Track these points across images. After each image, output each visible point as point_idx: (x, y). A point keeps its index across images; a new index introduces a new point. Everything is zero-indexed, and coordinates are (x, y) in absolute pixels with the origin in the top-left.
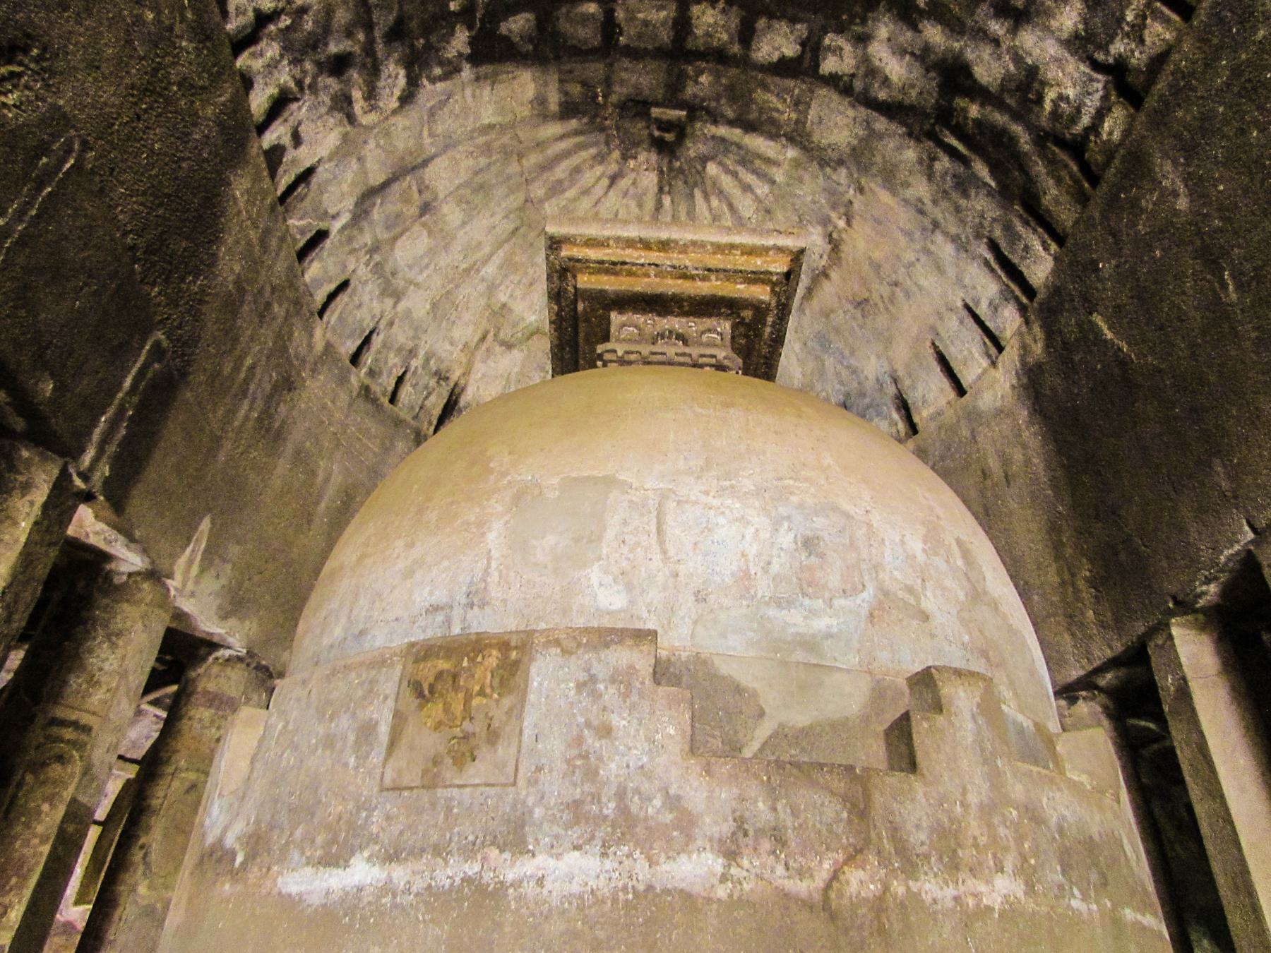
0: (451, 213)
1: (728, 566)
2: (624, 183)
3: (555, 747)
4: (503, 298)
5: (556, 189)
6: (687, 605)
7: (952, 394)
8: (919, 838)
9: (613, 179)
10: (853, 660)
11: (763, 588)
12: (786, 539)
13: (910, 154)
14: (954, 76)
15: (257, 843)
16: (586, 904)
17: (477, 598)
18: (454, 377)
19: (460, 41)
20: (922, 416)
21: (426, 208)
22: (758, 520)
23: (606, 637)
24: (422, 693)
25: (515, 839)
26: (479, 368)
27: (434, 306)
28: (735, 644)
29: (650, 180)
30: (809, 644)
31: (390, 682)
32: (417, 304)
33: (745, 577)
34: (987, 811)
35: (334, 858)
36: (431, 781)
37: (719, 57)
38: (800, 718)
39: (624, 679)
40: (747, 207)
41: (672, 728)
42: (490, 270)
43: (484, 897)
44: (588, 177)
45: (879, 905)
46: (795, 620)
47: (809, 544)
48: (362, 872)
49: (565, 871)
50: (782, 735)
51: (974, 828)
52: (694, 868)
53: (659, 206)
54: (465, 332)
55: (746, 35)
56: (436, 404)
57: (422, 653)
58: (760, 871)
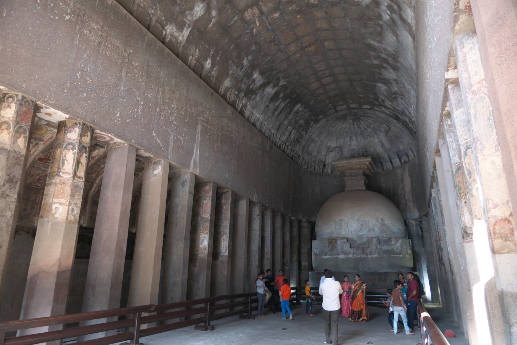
0: (317, 139)
1: (354, 229)
2: (346, 122)
3: (340, 248)
4: (328, 145)
5: (333, 127)
6: (350, 233)
7: (413, 157)
8: (368, 253)
9: (343, 123)
10: (365, 237)
11: (357, 231)
12: (359, 225)
13: (395, 121)
14: (396, 116)
15: (320, 254)
16: (343, 258)
17: (332, 233)
18: (324, 160)
19: (312, 123)
20: (410, 158)
21: (313, 141)
22: (357, 223)
23: (343, 238)
24: (330, 243)
25: (338, 254)
26: (327, 157)
27: (317, 152)
28: (355, 236)
29: (351, 121)
30: (361, 235)
31: (327, 242)
32: (315, 153)
33: (355, 230)
34: (375, 250)
35: (326, 255)
36: (332, 250)
37: (357, 108)
38: (360, 242)
39: (344, 242)
40: (370, 122)
41: (348, 246)
42: (325, 142)
43: (336, 258)
44: (339, 124)
45: (364, 258)
46: (360, 233)
47: (362, 225)
48: (328, 257)
49: (342, 256)
50: (359, 244)
51: (374, 251)
52: (351, 256)
53: (354, 123)
54: (323, 153)
55: (360, 106)
56: (322, 166)
57: (329, 240)
58: (356, 256)
